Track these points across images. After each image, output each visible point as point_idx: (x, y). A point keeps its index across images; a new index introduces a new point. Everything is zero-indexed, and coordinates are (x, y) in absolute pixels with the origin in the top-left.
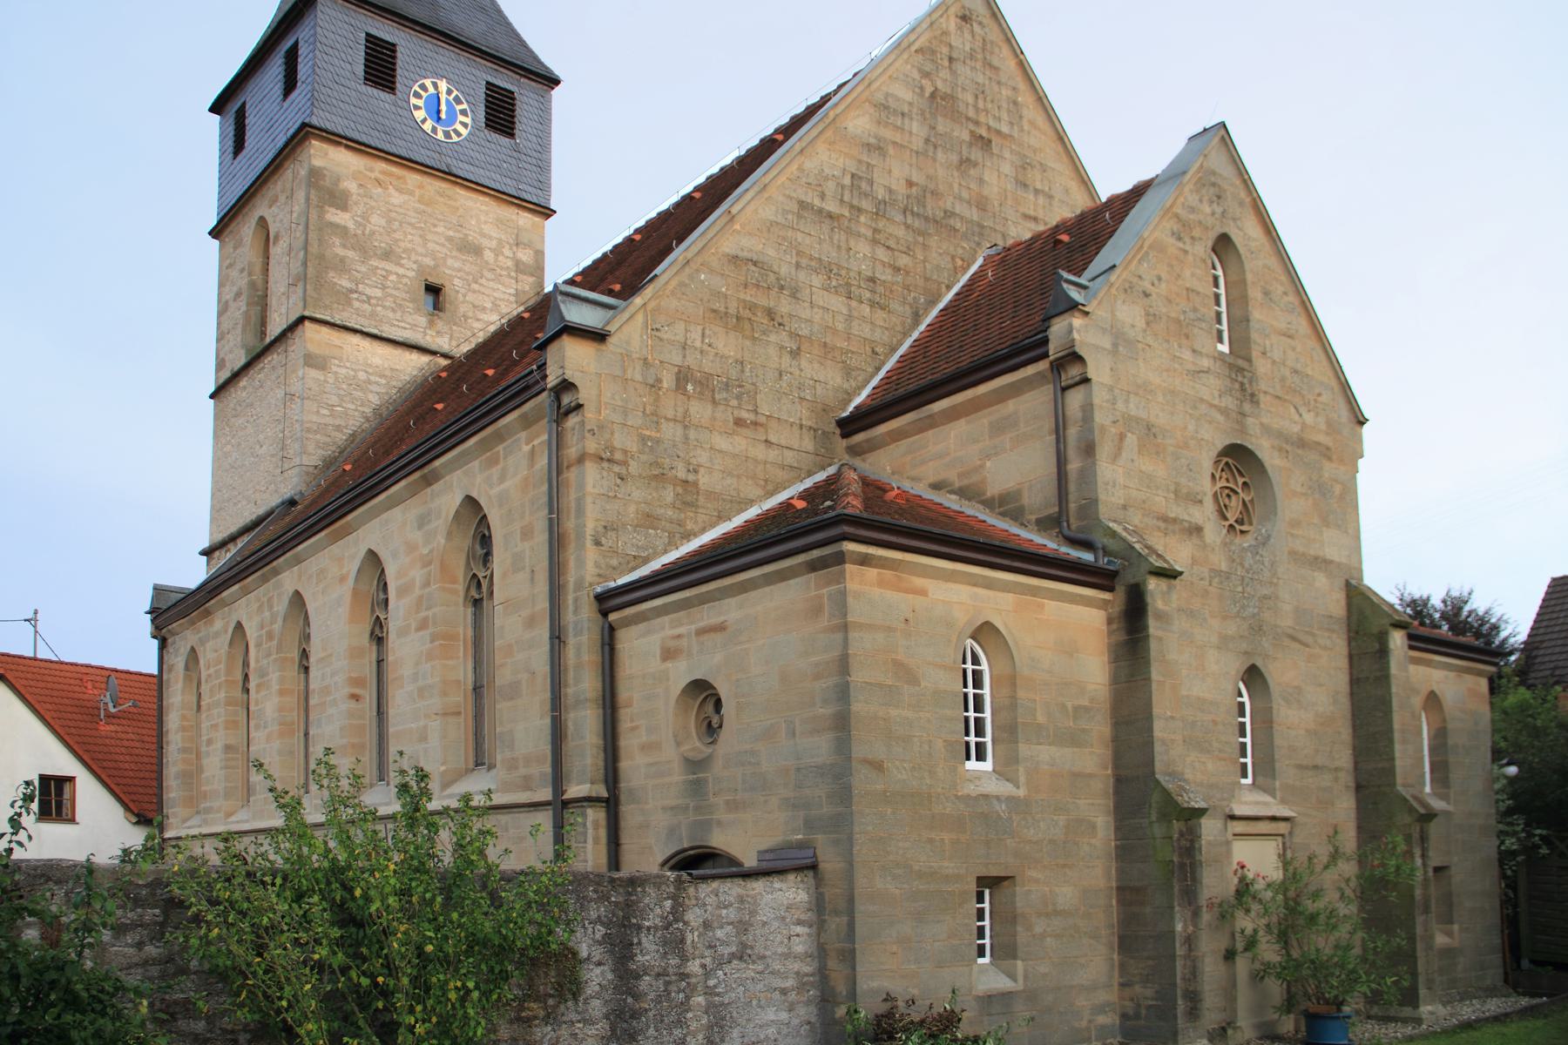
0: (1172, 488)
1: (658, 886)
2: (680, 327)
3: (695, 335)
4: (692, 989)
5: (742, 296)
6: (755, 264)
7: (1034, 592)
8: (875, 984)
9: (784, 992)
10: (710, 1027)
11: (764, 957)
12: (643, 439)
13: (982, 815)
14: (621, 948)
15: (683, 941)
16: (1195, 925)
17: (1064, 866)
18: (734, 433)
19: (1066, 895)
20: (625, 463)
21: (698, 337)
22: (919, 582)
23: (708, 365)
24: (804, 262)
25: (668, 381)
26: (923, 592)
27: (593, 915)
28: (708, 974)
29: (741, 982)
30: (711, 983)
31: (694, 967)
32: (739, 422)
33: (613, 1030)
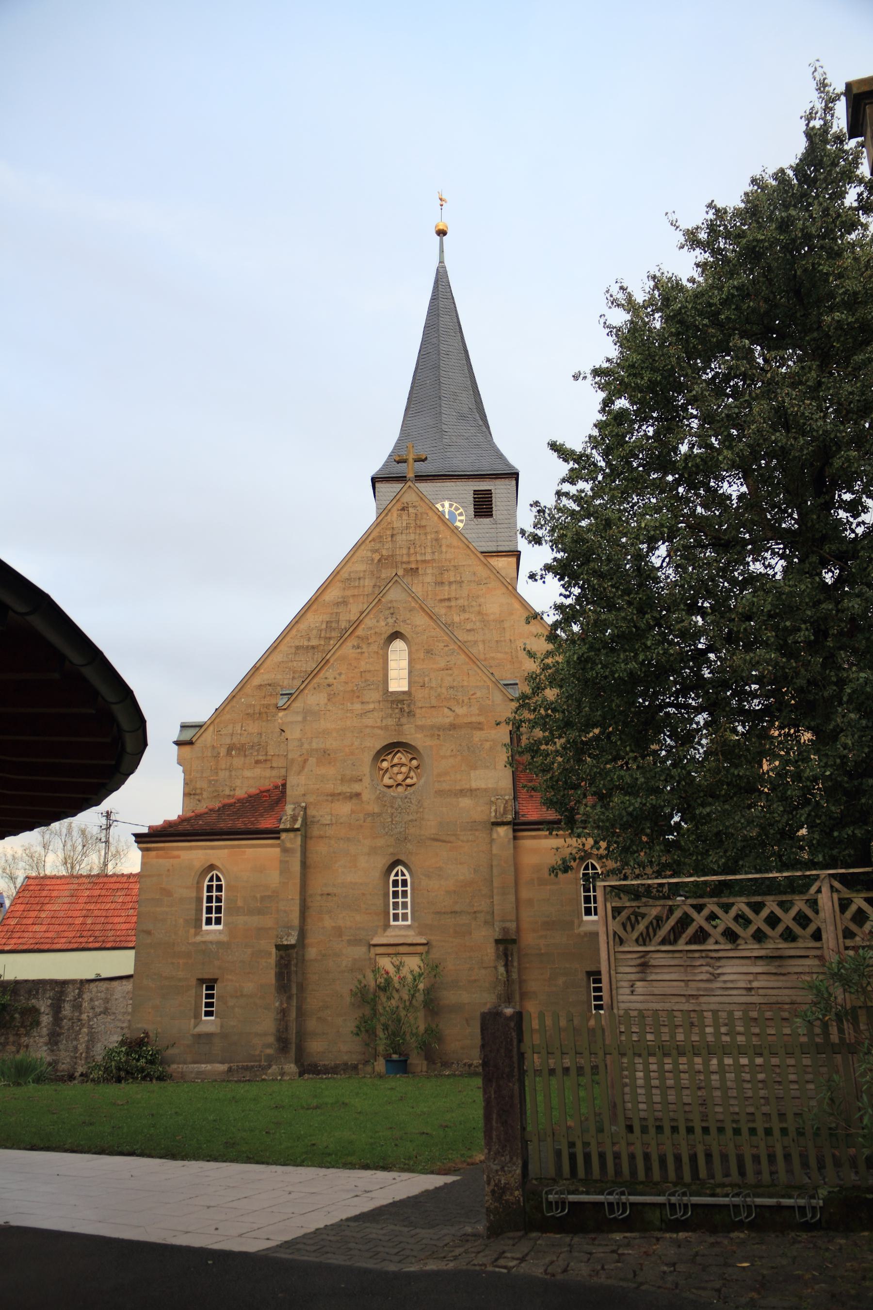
0: (340, 777)
1: (73, 984)
2: (230, 727)
3: (238, 728)
4: (83, 1026)
5: (263, 702)
6: (270, 685)
7: (239, 846)
8: (139, 1026)
9: (122, 1028)
10: (88, 1041)
11: (114, 1013)
12: (210, 781)
13: (205, 950)
14: (56, 1008)
15: (81, 1006)
16: (288, 1003)
17: (249, 973)
18: (255, 767)
19: (249, 987)
20: (201, 794)
21: (239, 728)
22: (176, 853)
23: (243, 740)
24: (297, 675)
25: (223, 751)
26: (178, 857)
27: (48, 996)
28: (90, 1019)
29: (104, 1023)
30: (91, 1023)
31: (84, 1017)
32: (257, 762)
33: (50, 1040)
